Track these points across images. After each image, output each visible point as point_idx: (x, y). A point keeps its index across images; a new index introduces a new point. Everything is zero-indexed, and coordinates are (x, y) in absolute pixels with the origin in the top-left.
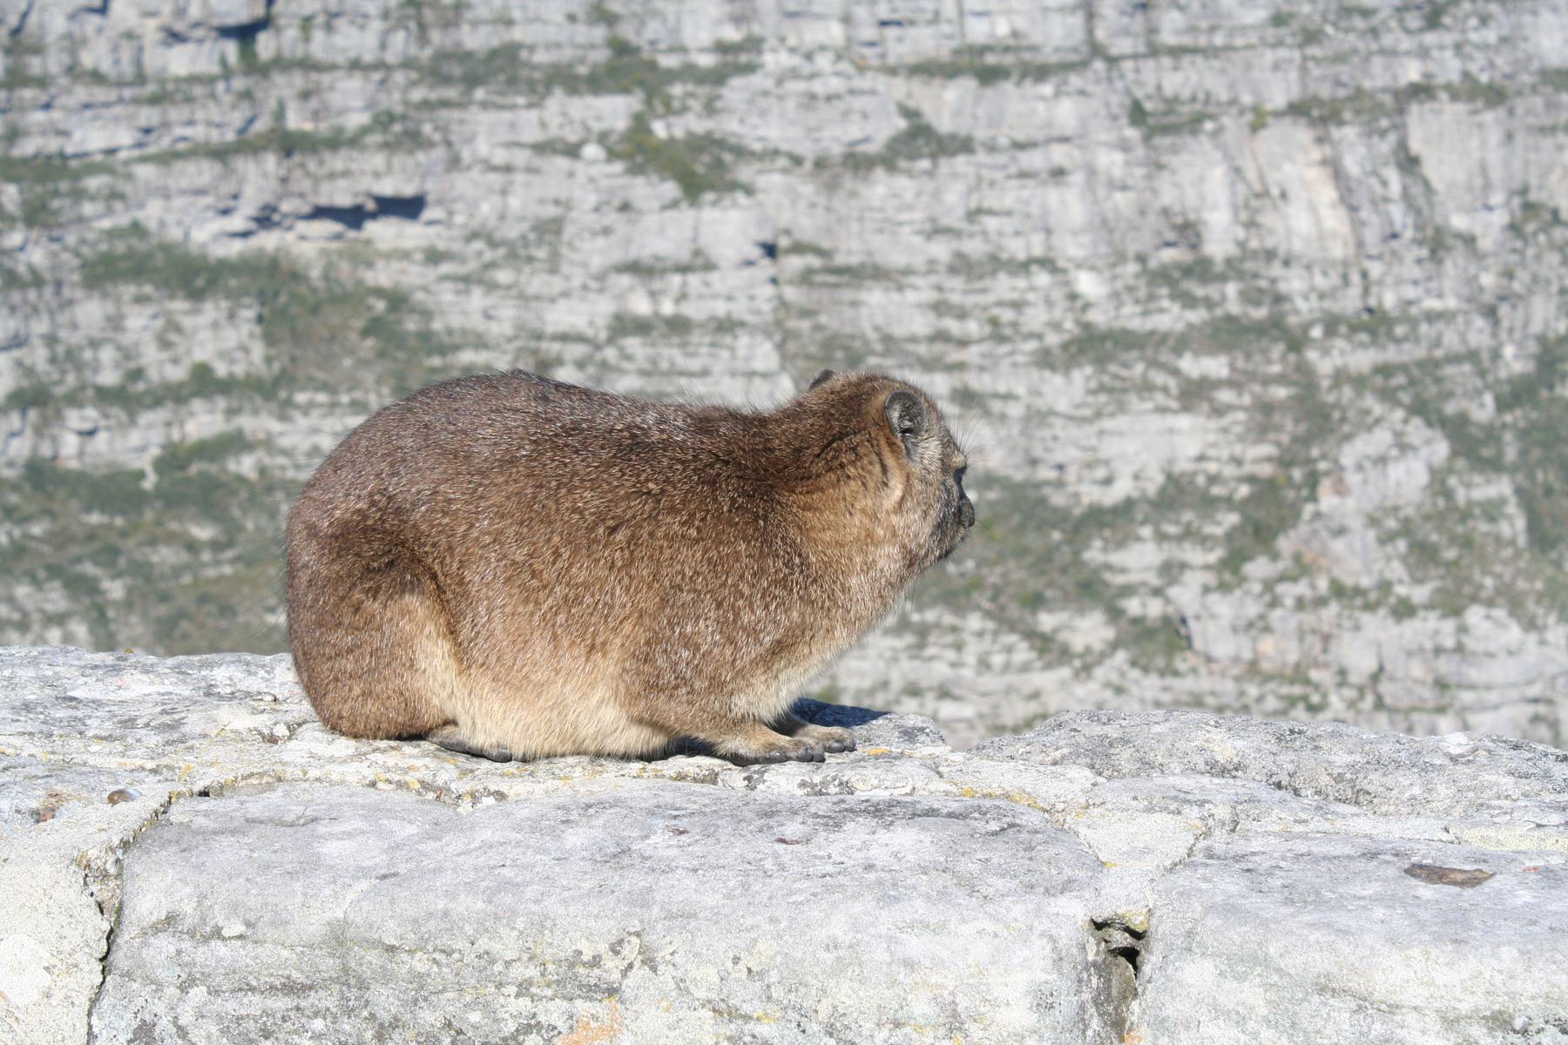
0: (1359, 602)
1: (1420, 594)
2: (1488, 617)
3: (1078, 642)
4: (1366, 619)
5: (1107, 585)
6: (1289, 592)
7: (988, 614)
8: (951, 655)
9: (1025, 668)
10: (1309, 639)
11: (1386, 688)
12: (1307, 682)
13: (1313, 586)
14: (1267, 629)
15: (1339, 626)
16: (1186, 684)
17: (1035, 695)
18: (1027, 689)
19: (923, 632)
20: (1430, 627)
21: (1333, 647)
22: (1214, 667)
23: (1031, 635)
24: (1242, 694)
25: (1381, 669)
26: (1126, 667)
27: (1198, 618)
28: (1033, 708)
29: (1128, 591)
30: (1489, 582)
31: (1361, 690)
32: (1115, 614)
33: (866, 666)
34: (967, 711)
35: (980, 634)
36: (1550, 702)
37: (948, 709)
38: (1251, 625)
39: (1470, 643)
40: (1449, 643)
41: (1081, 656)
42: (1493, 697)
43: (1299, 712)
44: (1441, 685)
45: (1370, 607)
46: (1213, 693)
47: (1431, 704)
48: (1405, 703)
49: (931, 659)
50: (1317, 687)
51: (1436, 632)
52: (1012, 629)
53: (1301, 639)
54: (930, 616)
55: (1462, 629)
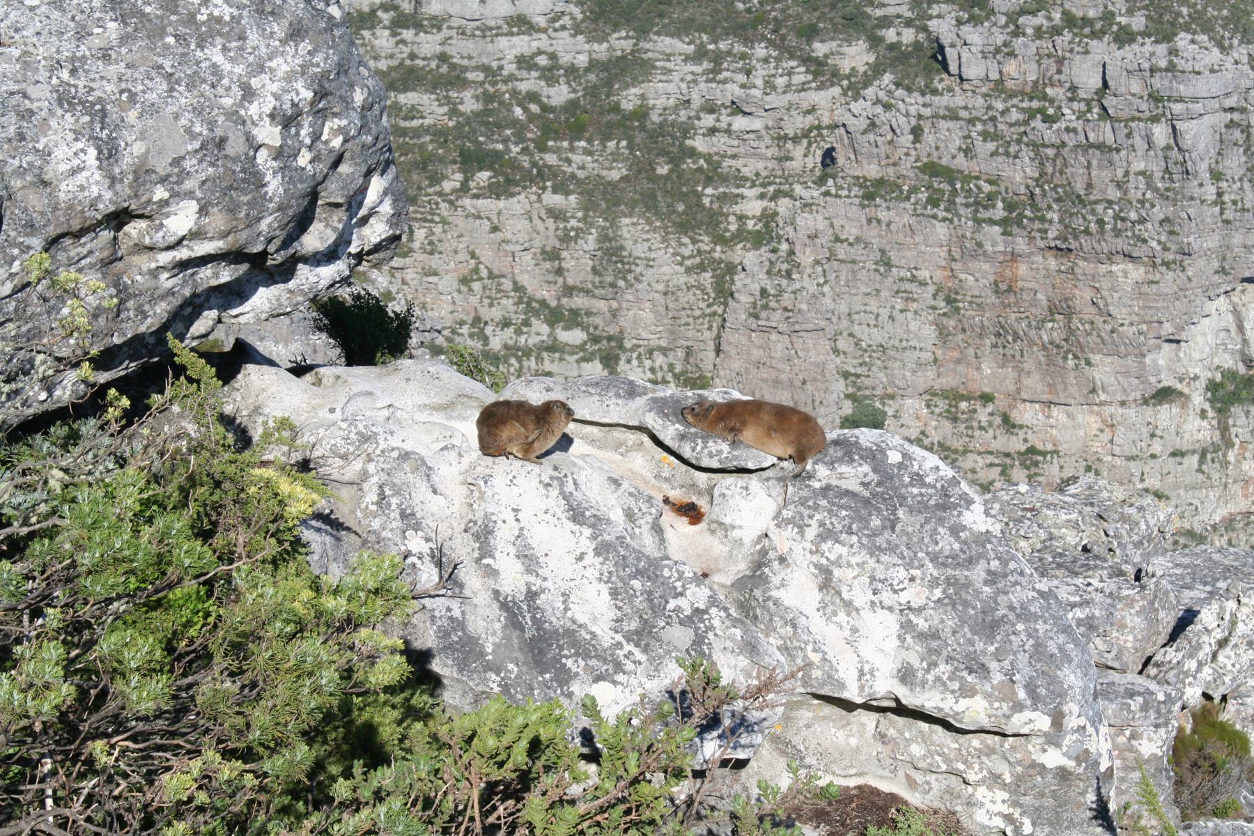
0: (1087, 30)
1: (1138, 22)
2: (1193, 42)
3: (845, 66)
4: (1094, 44)
5: (869, 17)
6: (1029, 23)
7: (771, 43)
8: (741, 78)
9: (803, 88)
10: (1045, 61)
11: (1109, 102)
12: (1044, 97)
13: (1050, 19)
14: (1012, 54)
15: (1071, 51)
16: (943, 101)
17: (812, 110)
18: (805, 106)
19: (717, 58)
20: (1148, 51)
21: (1065, 69)
22: (966, 86)
23: (807, 60)
24: (989, 108)
25: (1105, 85)
26: (892, 87)
27: (953, 46)
28: (810, 120)
29: (886, 22)
30: (1185, 10)
31: (1088, 103)
32: (875, 42)
33: (671, 88)
34: (757, 124)
35: (766, 61)
36: (1243, 110)
37: (740, 123)
38: (998, 51)
39: (1180, 64)
40: (1163, 64)
41: (848, 77)
42: (1198, 108)
43: (1037, 123)
44: (1155, 98)
45: (1095, 35)
46: (966, 108)
47: (1148, 114)
48: (1124, 115)
49: (725, 82)
50: (1052, 101)
51: (1153, 54)
52: (792, 57)
53: (1039, 63)
54: (723, 46)
55: (1173, 52)
